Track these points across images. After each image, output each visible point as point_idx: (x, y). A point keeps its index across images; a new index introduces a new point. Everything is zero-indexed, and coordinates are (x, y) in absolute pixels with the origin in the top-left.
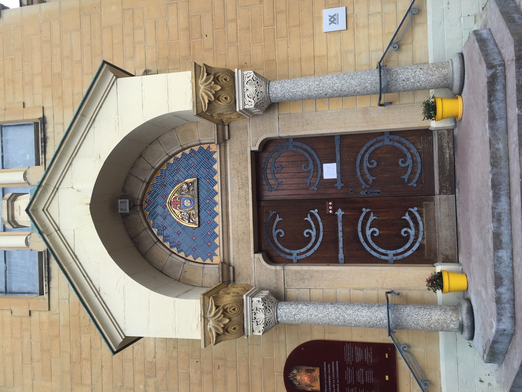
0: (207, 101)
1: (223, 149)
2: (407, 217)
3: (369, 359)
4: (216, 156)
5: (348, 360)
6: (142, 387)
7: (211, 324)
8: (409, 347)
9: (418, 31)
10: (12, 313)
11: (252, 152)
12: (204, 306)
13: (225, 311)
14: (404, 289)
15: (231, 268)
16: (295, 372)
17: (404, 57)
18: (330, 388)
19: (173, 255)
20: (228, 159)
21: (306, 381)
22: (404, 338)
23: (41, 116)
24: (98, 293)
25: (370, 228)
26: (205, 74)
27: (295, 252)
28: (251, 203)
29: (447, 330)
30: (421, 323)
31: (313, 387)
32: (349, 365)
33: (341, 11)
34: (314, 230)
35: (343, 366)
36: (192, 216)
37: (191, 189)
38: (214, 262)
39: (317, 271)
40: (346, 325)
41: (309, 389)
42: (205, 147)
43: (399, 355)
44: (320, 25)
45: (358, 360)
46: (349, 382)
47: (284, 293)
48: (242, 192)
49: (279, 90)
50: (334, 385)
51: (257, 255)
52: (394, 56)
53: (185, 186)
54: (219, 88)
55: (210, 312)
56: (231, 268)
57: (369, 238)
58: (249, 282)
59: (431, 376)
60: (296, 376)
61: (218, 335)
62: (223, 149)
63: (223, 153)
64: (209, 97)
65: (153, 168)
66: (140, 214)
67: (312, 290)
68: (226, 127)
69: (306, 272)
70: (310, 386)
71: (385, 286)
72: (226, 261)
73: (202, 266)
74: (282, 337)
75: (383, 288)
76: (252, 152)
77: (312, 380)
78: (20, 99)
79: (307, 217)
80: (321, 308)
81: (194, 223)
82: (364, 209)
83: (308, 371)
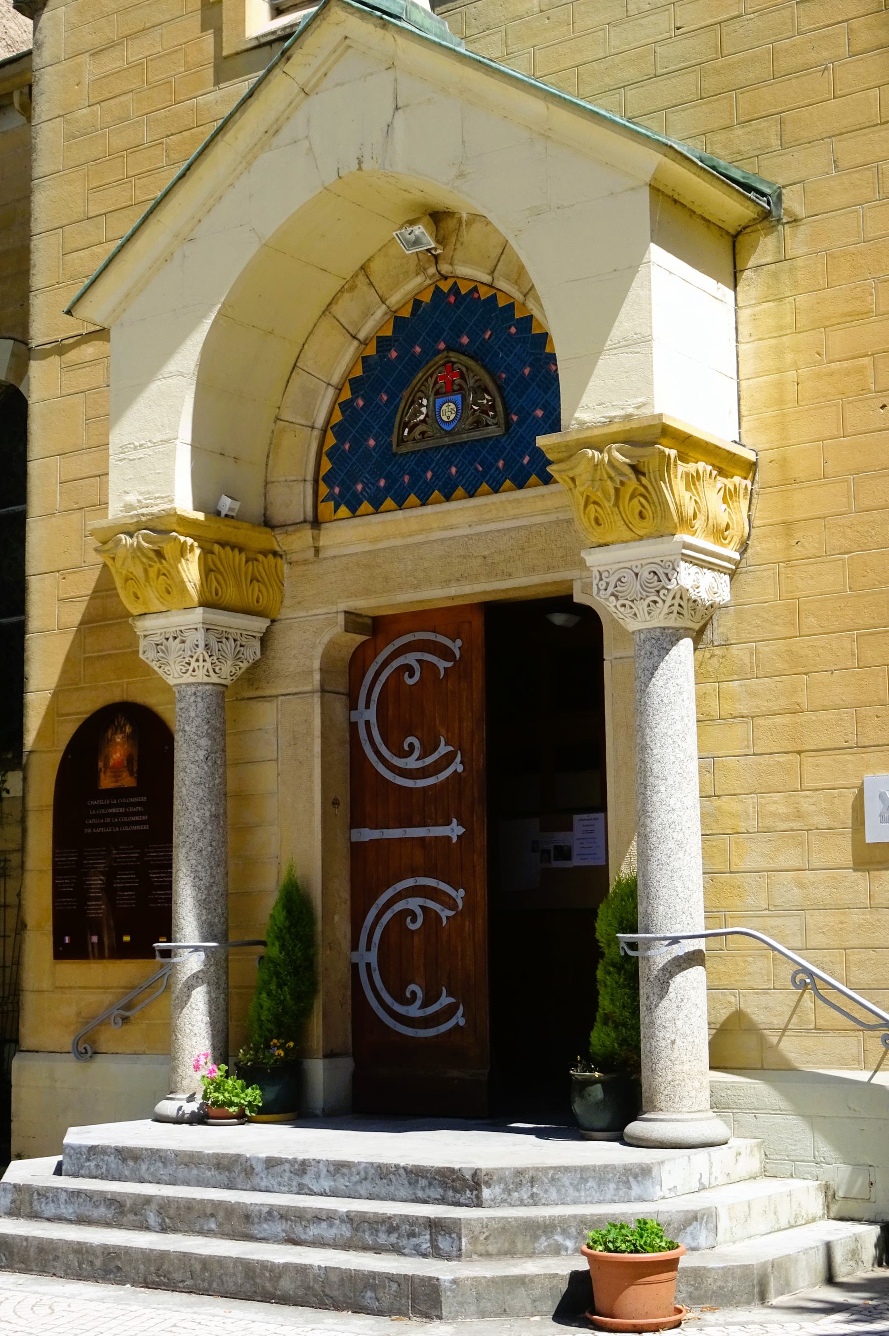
2: (445, 1000)
18: (103, 811)
21: (114, 756)
25: (423, 908)
27: (371, 715)
31: (105, 773)
34: (420, 764)
38: (321, 507)
39: (310, 776)
41: (101, 765)
47: (274, 692)
50: (109, 820)
58: (287, 602)
60: (122, 732)
66: (419, 279)
67: (274, 764)
73: (310, 476)
79: (447, 744)
82: (462, 892)
83: (130, 759)
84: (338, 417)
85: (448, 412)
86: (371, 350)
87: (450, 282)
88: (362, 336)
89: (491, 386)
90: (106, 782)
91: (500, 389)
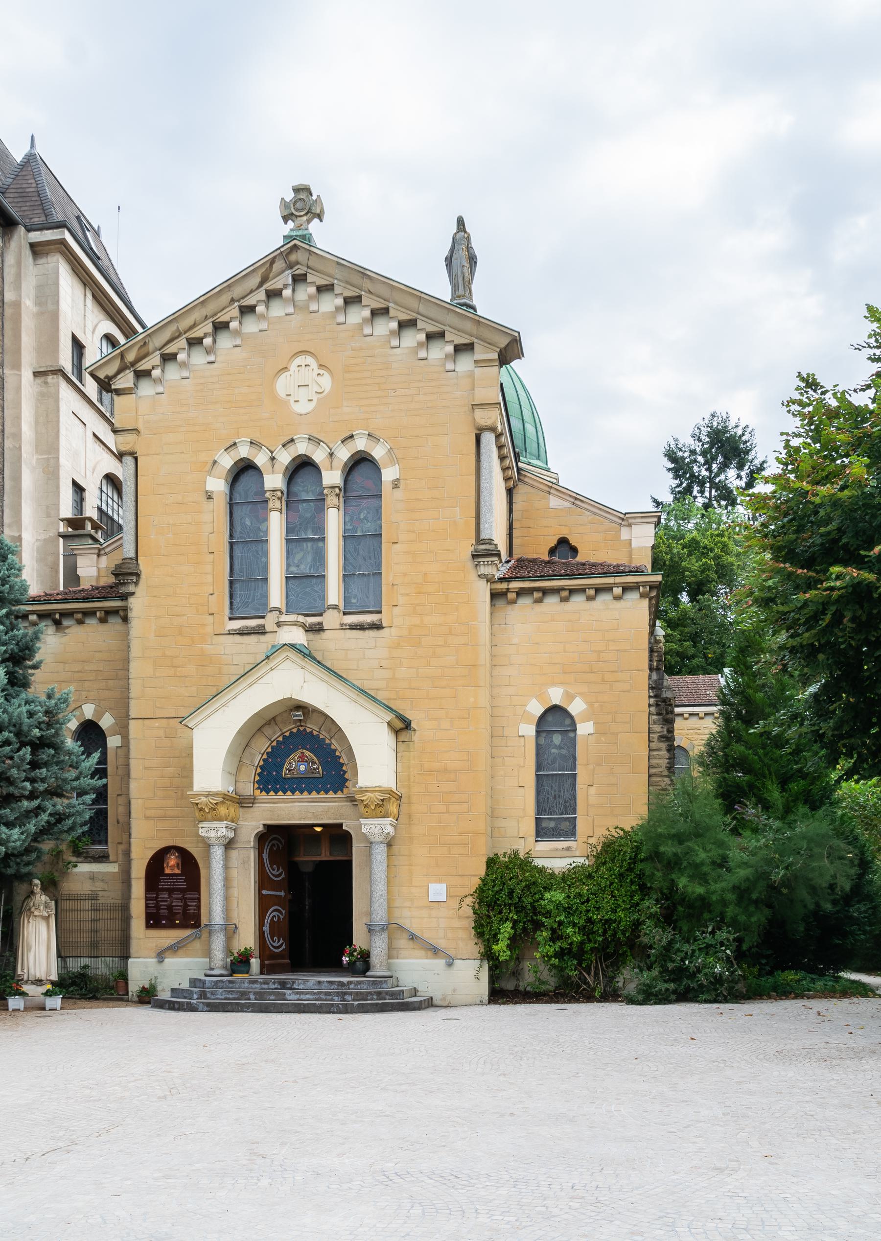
0: (362, 799)
4: (339, 795)
5: (188, 895)
6: (157, 724)
8: (199, 938)
9: (422, 953)
10: (211, 594)
11: (341, 825)
14: (239, 935)
15: (251, 805)
16: (177, 854)
17: (402, 942)
19: (260, 755)
20: (337, 804)
28: (302, 822)
29: (210, 962)
30: (213, 944)
32: (184, 895)
33: (444, 898)
40: (210, 895)
41: (165, 865)
43: (194, 930)
44: (436, 882)
48: (310, 815)
51: (262, 826)
52: (405, 935)
53: (315, 766)
56: (251, 805)
57: (272, 915)
58: (241, 819)
59: (180, 952)
62: (344, 799)
63: (342, 799)
71: (241, 923)
72: (256, 801)
73: (252, 781)
76: (341, 825)
77: (172, 868)
80: (221, 878)
81: (286, 774)
83: (178, 864)
84: (262, 763)
85: (302, 768)
86: (274, 744)
87: (303, 728)
89: (317, 762)
90: (168, 871)
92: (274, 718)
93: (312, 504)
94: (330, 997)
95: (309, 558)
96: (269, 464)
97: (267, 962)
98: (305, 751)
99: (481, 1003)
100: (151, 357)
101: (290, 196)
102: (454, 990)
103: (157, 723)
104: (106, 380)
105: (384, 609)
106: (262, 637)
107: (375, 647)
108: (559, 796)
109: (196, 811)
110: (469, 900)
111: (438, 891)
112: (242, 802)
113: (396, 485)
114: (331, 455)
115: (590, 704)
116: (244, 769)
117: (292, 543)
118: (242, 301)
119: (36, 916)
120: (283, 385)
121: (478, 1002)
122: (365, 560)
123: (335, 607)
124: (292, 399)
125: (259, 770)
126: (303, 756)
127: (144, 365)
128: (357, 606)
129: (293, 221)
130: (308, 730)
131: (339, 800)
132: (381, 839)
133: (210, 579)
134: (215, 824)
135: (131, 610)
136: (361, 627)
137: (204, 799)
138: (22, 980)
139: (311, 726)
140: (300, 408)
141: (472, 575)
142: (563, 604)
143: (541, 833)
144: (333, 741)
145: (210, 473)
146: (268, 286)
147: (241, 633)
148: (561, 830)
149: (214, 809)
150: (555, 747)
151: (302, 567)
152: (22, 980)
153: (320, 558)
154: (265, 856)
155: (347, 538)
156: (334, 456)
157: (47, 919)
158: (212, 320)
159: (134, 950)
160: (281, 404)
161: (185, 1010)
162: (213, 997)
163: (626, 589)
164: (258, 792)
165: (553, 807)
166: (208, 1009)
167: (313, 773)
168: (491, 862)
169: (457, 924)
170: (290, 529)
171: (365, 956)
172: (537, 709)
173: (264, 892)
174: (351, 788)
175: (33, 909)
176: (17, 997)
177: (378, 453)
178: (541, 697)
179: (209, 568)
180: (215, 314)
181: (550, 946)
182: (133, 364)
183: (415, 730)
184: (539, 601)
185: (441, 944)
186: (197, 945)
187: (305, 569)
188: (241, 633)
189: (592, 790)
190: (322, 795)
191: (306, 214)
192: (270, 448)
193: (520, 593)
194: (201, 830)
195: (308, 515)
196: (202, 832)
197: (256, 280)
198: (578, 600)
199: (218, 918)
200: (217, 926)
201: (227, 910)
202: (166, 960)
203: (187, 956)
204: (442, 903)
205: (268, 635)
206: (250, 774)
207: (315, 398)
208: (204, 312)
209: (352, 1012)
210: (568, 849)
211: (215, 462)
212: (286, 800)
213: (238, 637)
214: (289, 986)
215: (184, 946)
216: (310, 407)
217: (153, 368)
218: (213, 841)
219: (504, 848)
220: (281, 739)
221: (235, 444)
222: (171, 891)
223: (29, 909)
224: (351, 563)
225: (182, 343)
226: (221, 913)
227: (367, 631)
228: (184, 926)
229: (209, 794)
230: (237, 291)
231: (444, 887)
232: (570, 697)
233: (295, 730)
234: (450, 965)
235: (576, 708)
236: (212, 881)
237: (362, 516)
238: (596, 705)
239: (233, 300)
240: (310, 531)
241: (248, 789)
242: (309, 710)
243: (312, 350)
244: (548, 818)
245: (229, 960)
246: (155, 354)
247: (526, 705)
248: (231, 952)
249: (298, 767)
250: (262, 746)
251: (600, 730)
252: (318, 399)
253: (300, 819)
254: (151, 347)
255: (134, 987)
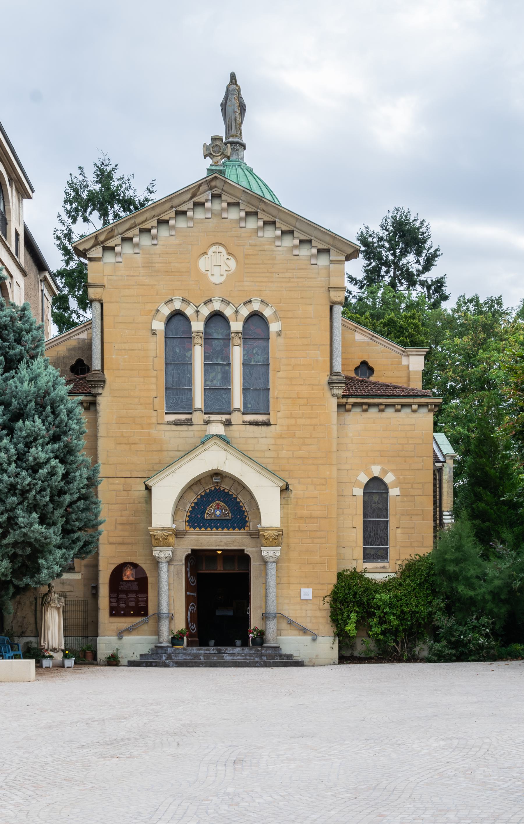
1: (246, 534)
3: (140, 604)
4: (242, 531)
5: (139, 595)
7: (159, 532)
8: (147, 623)
9: (296, 632)
10: (156, 397)
11: (243, 550)
12: (168, 529)
13: (166, 539)
14: (174, 621)
15: (183, 536)
17: (284, 625)
19: (190, 504)
20: (241, 536)
22: (151, 621)
23: (271, 423)
24: (173, 472)
26: (277, 534)
29: (158, 638)
30: (162, 627)
32: (137, 595)
33: (310, 597)
35: (136, 592)
36: (211, 515)
37: (226, 515)
39: (182, 581)
40: (158, 595)
42: (247, 524)
43: (143, 618)
44: (305, 587)
45: (140, 599)
46: (129, 594)
48: (223, 543)
49: (270, 567)
51: (190, 550)
52: (285, 621)
54: (271, 540)
55: (165, 532)
56: (183, 536)
58: (176, 545)
59: (134, 632)
61: (155, 536)
62: (246, 534)
64: (267, 535)
65: (238, 494)
66: (212, 486)
68: (257, 536)
69: (182, 575)
70: (125, 575)
71: (176, 613)
72: (187, 534)
73: (184, 521)
74: (148, 562)
75: (174, 612)
76: (243, 550)
77: (128, 577)
78: (283, 408)
80: (167, 583)
81: (207, 517)
83: (132, 574)
84: (191, 509)
85: (218, 513)
86: (199, 497)
88: (198, 494)
90: (125, 578)
91: (230, 510)
92: (199, 481)
93: (221, 341)
94: (253, 658)
95: (220, 377)
96: (195, 315)
97: (189, 639)
98: (220, 502)
99: (334, 664)
100: (115, 238)
101: (209, 142)
102: (317, 656)
103: (117, 481)
104: (84, 251)
105: (271, 412)
106: (190, 428)
107: (266, 437)
108: (377, 534)
109: (153, 540)
110: (328, 599)
111: (307, 593)
112: (178, 534)
113: (279, 334)
114: (237, 312)
115: (397, 477)
116: (179, 513)
117: (208, 367)
118: (178, 208)
119: (52, 607)
120: (203, 264)
121: (332, 663)
122: (257, 380)
123: (239, 410)
124: (209, 273)
125: (189, 514)
126: (218, 505)
127: (110, 243)
128: (251, 409)
129: (212, 159)
130: (222, 489)
131: (243, 534)
132: (274, 560)
133: (154, 387)
134: (165, 548)
135: (99, 404)
136: (256, 424)
137: (159, 532)
138: (44, 648)
139: (225, 486)
140: (217, 279)
141: (328, 394)
142: (380, 413)
143: (367, 556)
144: (239, 496)
145: (154, 317)
146: (195, 199)
147: (176, 423)
148: (378, 555)
149: (166, 539)
150: (375, 503)
151: (215, 382)
152: (44, 648)
153: (227, 377)
154: (188, 569)
155: (246, 365)
156: (238, 313)
157: (58, 609)
158: (157, 218)
159: (100, 631)
160: (202, 277)
161: (160, 666)
162: (176, 659)
163: (420, 406)
164: (188, 528)
165: (373, 541)
166: (176, 665)
167: (225, 516)
168: (340, 576)
169: (319, 614)
170: (206, 357)
171: (261, 634)
172: (364, 479)
173: (188, 593)
174: (251, 526)
175: (51, 602)
176: (48, 659)
177: (267, 313)
178: (367, 471)
179: (154, 380)
180: (160, 215)
181: (378, 627)
182: (102, 242)
183: (292, 491)
184: (366, 410)
185: (309, 626)
186: (145, 627)
187: (217, 383)
188: (176, 423)
189: (399, 531)
190: (231, 531)
191: (221, 155)
192: (195, 304)
193: (354, 405)
194: (154, 552)
195: (219, 348)
196: (155, 554)
197: (189, 195)
198: (390, 411)
199: (164, 609)
200: (164, 615)
201: (169, 605)
202: (124, 637)
203: (138, 635)
204: (309, 601)
205: (194, 426)
206: (184, 516)
207: (225, 274)
208: (153, 213)
209: (269, 667)
210: (384, 567)
211: (158, 311)
212: (207, 534)
213: (173, 427)
214: (223, 651)
215: (136, 629)
216: (222, 279)
217: (116, 245)
218: (162, 560)
219: (349, 566)
220: (203, 494)
221: (172, 300)
222: (127, 592)
223: (49, 602)
224: (247, 382)
225: (136, 231)
226: (166, 607)
227: (260, 427)
228: (137, 614)
229: (163, 529)
230: (176, 202)
231: (309, 591)
232: (385, 472)
233: (213, 489)
234: (314, 640)
235: (389, 479)
236: (161, 586)
237: (255, 351)
238: (401, 477)
239: (172, 207)
240: (219, 359)
241: (183, 526)
242: (223, 476)
243: (223, 243)
244: (370, 548)
245: (170, 637)
246: (117, 237)
247: (357, 476)
248: (171, 632)
249: (214, 512)
250: (192, 498)
251: (404, 493)
252: (227, 275)
253: (216, 546)
254: (116, 232)
255: (102, 655)
